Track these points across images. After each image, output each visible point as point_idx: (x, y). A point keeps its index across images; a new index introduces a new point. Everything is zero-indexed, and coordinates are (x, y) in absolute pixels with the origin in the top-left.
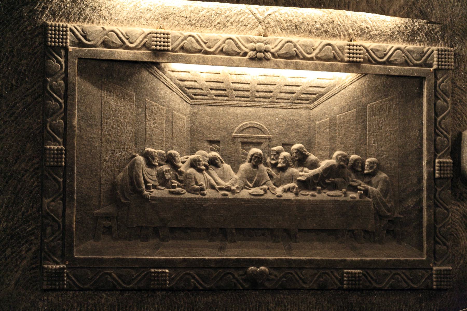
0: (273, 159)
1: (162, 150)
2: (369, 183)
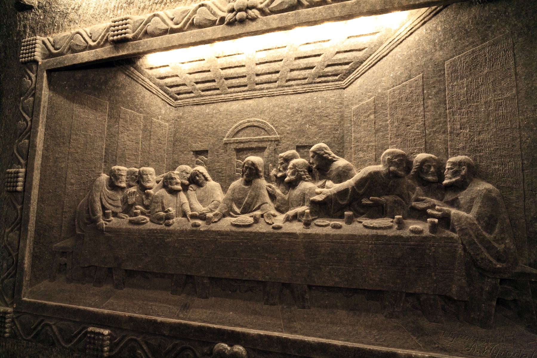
0: (280, 171)
1: (136, 167)
2: (454, 203)
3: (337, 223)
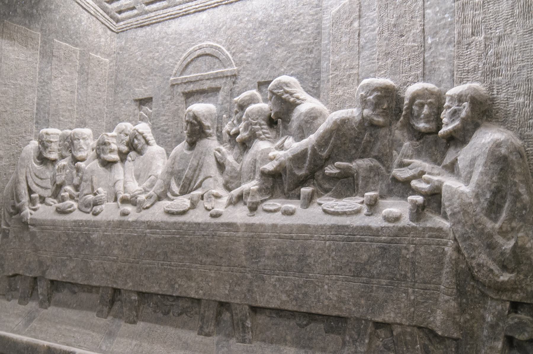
2: (452, 168)
3: (290, 205)
